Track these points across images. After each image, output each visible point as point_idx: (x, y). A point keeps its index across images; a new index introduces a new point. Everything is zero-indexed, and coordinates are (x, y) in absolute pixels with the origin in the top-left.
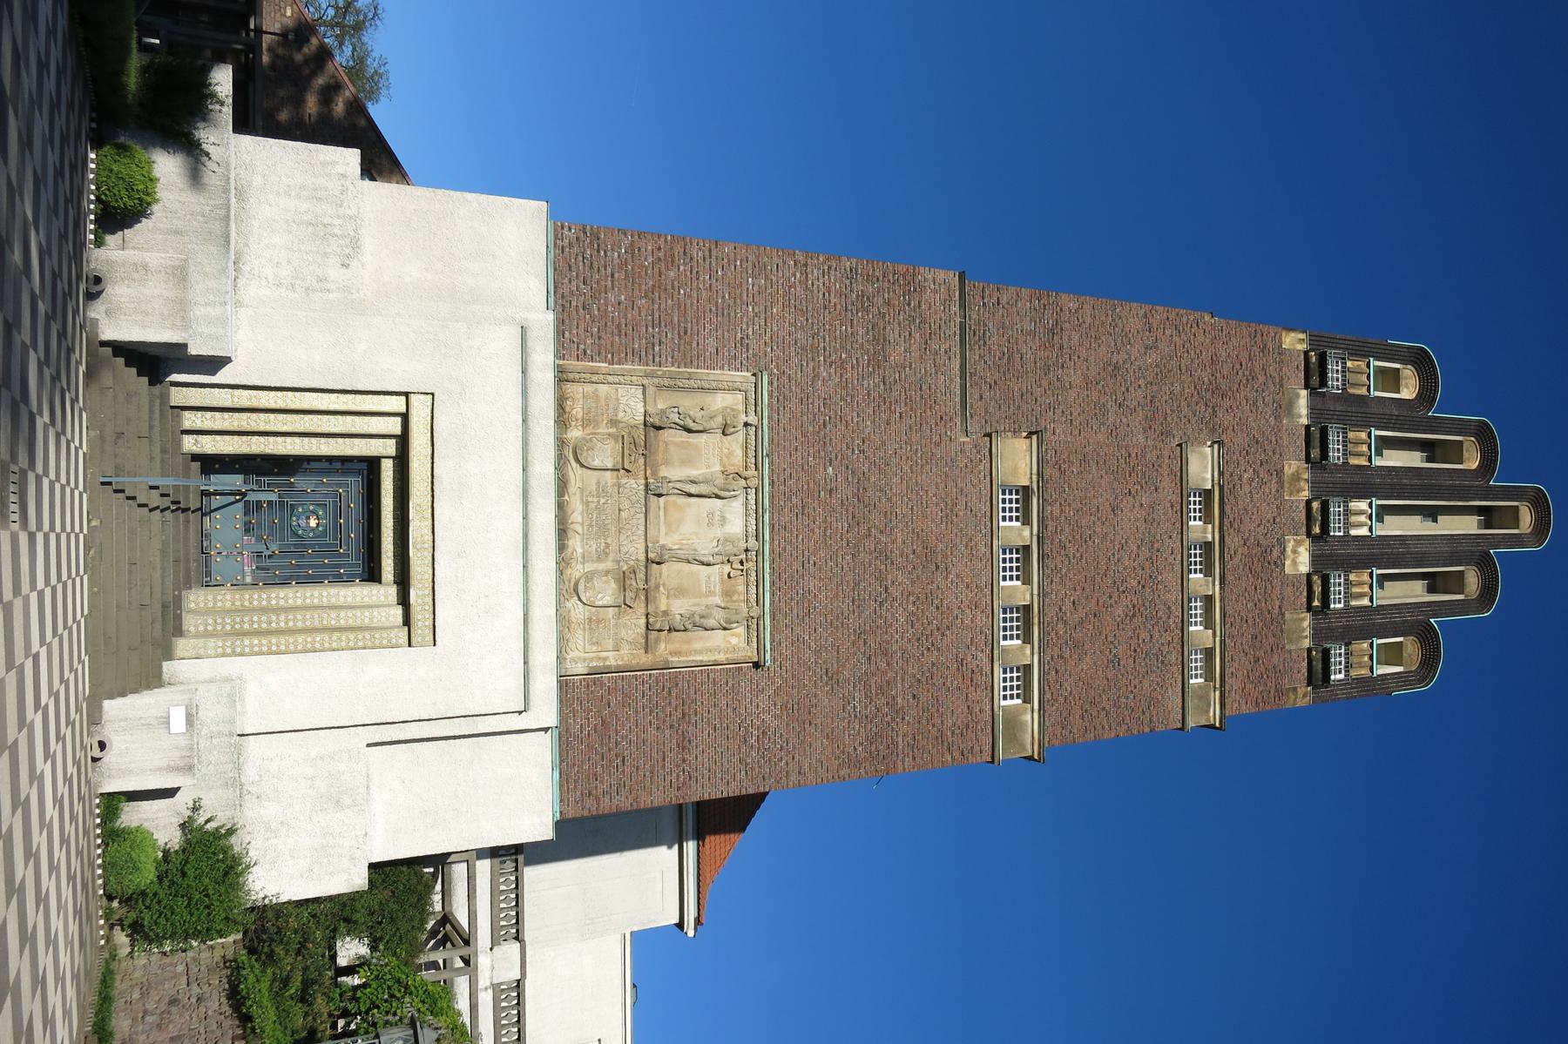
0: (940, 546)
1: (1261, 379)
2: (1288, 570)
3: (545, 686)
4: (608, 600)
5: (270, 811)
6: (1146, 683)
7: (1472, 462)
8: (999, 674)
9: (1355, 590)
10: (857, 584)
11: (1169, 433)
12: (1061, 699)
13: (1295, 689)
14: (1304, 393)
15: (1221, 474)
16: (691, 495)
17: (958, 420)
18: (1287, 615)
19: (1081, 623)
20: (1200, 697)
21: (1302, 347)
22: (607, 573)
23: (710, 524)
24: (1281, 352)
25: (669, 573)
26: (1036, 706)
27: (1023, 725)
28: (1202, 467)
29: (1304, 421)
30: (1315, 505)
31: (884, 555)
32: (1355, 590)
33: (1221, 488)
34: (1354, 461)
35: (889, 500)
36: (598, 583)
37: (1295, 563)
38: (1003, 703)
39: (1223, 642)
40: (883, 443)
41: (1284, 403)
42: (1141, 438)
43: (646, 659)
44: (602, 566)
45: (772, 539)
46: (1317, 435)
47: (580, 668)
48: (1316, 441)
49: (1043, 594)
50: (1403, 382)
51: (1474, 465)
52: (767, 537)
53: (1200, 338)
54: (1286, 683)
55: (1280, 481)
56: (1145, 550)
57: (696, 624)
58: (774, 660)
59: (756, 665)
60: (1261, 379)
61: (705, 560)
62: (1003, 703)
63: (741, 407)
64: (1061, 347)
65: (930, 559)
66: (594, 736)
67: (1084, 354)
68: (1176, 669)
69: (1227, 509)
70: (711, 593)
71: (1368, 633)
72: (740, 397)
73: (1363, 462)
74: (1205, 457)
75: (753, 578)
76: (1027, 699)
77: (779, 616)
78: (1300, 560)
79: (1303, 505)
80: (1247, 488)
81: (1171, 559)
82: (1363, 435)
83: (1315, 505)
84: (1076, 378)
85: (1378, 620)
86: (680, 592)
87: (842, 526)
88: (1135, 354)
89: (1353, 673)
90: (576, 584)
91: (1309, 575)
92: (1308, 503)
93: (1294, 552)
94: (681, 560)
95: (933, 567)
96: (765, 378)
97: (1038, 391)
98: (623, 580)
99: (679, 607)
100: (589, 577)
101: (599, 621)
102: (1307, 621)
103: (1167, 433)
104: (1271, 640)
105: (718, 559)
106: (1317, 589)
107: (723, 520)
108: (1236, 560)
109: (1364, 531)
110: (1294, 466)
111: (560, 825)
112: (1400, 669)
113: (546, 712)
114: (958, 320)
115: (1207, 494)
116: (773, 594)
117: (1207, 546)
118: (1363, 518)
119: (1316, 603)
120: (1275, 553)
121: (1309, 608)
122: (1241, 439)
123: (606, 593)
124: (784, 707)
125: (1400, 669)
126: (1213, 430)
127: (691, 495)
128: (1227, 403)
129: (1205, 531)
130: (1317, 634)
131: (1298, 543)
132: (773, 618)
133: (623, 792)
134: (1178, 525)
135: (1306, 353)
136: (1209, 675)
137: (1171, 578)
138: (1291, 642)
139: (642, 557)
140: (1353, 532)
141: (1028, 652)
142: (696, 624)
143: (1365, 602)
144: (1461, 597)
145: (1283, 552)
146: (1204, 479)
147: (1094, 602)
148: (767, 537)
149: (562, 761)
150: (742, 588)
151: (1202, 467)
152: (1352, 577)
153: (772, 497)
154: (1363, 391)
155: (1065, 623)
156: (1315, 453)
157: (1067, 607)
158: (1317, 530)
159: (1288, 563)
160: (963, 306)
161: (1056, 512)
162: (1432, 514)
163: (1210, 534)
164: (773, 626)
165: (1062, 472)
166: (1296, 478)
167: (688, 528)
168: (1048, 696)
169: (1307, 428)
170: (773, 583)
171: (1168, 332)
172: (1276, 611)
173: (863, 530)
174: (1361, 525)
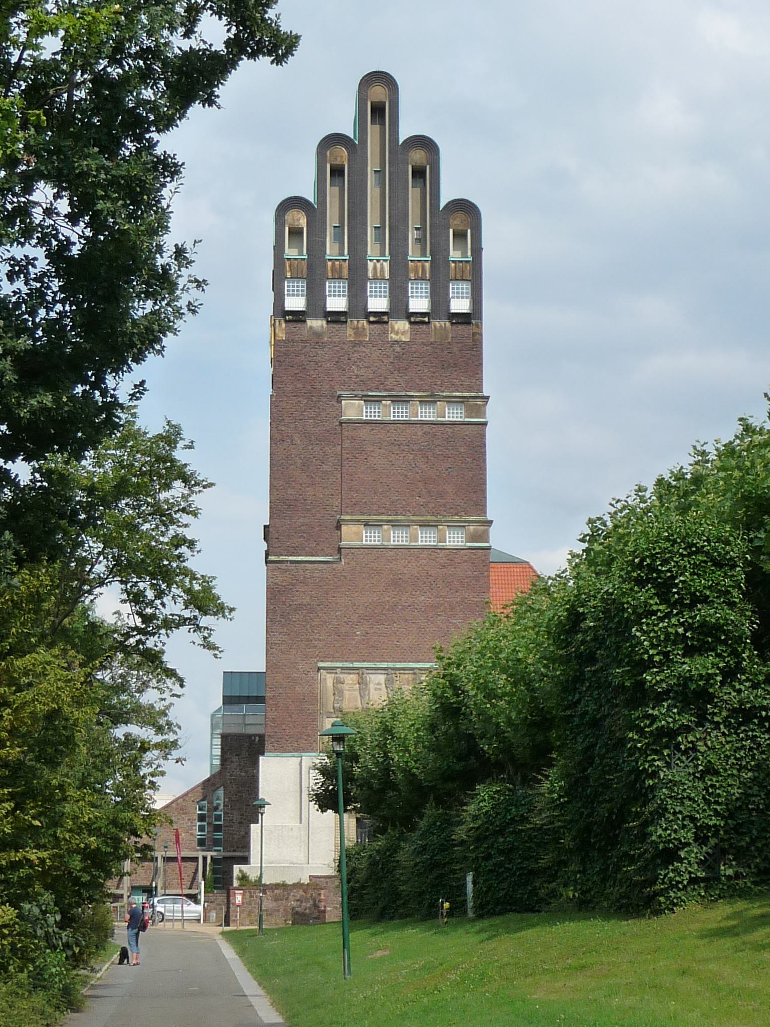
2: (405, 338)
15: (356, 396)
18: (432, 340)
21: (284, 325)
29: (324, 322)
30: (372, 319)
37: (403, 333)
52: (384, 665)
63: (333, 675)
72: (328, 675)
79: (372, 326)
80: (363, 371)
82: (330, 263)
91: (411, 323)
96: (321, 664)
104: (446, 352)
107: (379, 684)
109: (386, 265)
112: (469, 231)
118: (378, 265)
119: (426, 319)
120: (398, 349)
125: (469, 231)
129: (385, 406)
131: (393, 330)
135: (286, 321)
138: (447, 337)
146: (359, 405)
150: (406, 676)
157: (421, 501)
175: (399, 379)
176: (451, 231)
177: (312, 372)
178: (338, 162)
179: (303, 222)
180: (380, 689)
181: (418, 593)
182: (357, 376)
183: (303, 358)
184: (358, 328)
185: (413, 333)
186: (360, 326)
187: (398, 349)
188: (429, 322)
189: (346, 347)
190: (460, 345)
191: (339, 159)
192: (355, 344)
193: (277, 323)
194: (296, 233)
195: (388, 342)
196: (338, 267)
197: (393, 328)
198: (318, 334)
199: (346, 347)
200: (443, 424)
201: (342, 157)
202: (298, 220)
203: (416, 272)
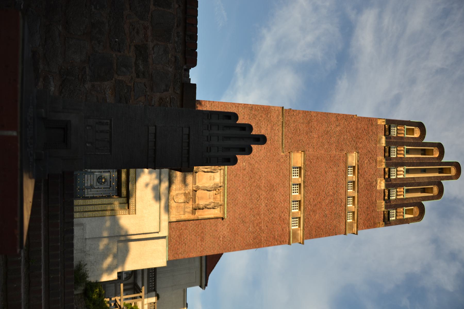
0: (275, 184)
2: (378, 188)
3: (165, 225)
4: (182, 201)
5: (92, 258)
6: (334, 222)
7: (436, 154)
8: (291, 220)
9: (399, 193)
10: (251, 195)
11: (343, 150)
12: (309, 227)
13: (379, 223)
14: (384, 137)
15: (358, 161)
16: (205, 172)
17: (281, 149)
18: (378, 201)
19: (315, 205)
21: (384, 123)
22: (182, 194)
23: (210, 179)
24: (377, 125)
25: (199, 193)
26: (302, 229)
27: (299, 233)
28: (353, 159)
30: (387, 169)
31: (259, 187)
32: (399, 193)
33: (358, 166)
34: (399, 156)
35: (261, 172)
36: (179, 197)
37: (380, 186)
38: (292, 228)
39: (358, 210)
40: (259, 156)
41: (378, 140)
42: (334, 152)
43: (192, 217)
44: (181, 192)
45: (227, 183)
46: (387, 150)
47: (174, 220)
48: (387, 150)
49: (304, 196)
50: (415, 132)
52: (226, 183)
53: (353, 122)
54: (377, 221)
55: (376, 162)
56: (335, 184)
57: (205, 207)
58: (227, 217)
59: (223, 219)
60: (371, 133)
61: (208, 189)
62: (292, 228)
64: (311, 127)
65: (271, 188)
66: (178, 238)
67: (318, 129)
68: (343, 218)
69: (360, 171)
70: (210, 198)
71: (402, 206)
73: (402, 156)
74: (353, 156)
75: (222, 194)
76: (299, 226)
77: (229, 205)
78: (382, 185)
79: (383, 170)
80: (366, 165)
81: (343, 186)
82: (402, 148)
83: (387, 169)
84: (315, 136)
85: (406, 202)
86: (202, 198)
87: (247, 179)
88: (333, 128)
89: (398, 218)
90: (173, 197)
91: (384, 190)
92: (384, 169)
93: (380, 183)
94: (202, 190)
95: (273, 190)
97: (304, 140)
98: (185, 194)
99: (202, 203)
100: (177, 195)
101: (179, 207)
102: (383, 203)
103: (342, 150)
105: (213, 189)
108: (362, 186)
109: (402, 176)
110: (381, 158)
111: (168, 262)
112: (412, 216)
113: (164, 232)
114: (281, 120)
115: (354, 167)
116: (227, 198)
117: (354, 182)
118: (402, 173)
119: (386, 198)
120: (374, 183)
121: (384, 199)
122: (365, 151)
123: (181, 199)
124: (230, 229)
126: (356, 149)
127: (205, 172)
128: (361, 140)
130: (386, 207)
131: (381, 180)
132: (227, 205)
133: (185, 253)
134: (345, 176)
135: (385, 125)
136: (353, 219)
137: (342, 191)
138: (378, 209)
139: (191, 189)
140: (399, 177)
141: (300, 213)
142: (205, 207)
143: (402, 197)
144: (432, 195)
145: (377, 183)
146: (353, 163)
147: (319, 199)
148: (226, 183)
149: (169, 244)
151: (353, 159)
152: (398, 190)
153: (228, 172)
154: (403, 135)
155: (311, 205)
156: (387, 154)
157: (312, 200)
158: (387, 177)
159: (378, 186)
160: (283, 116)
161: (309, 174)
162: (424, 171)
163: (355, 179)
164: (227, 207)
165: (311, 162)
166: (381, 161)
167: (204, 181)
168: (306, 226)
169: (385, 147)
170: (227, 195)
171: (343, 121)
172: (374, 200)
173: (253, 180)
174: (401, 174)
175: (363, 185)
176: (413, 207)
177: (365, 138)
178: (434, 153)
180: (210, 179)
181: (266, 202)
182: (364, 162)
185: (379, 192)
194: (411, 131)
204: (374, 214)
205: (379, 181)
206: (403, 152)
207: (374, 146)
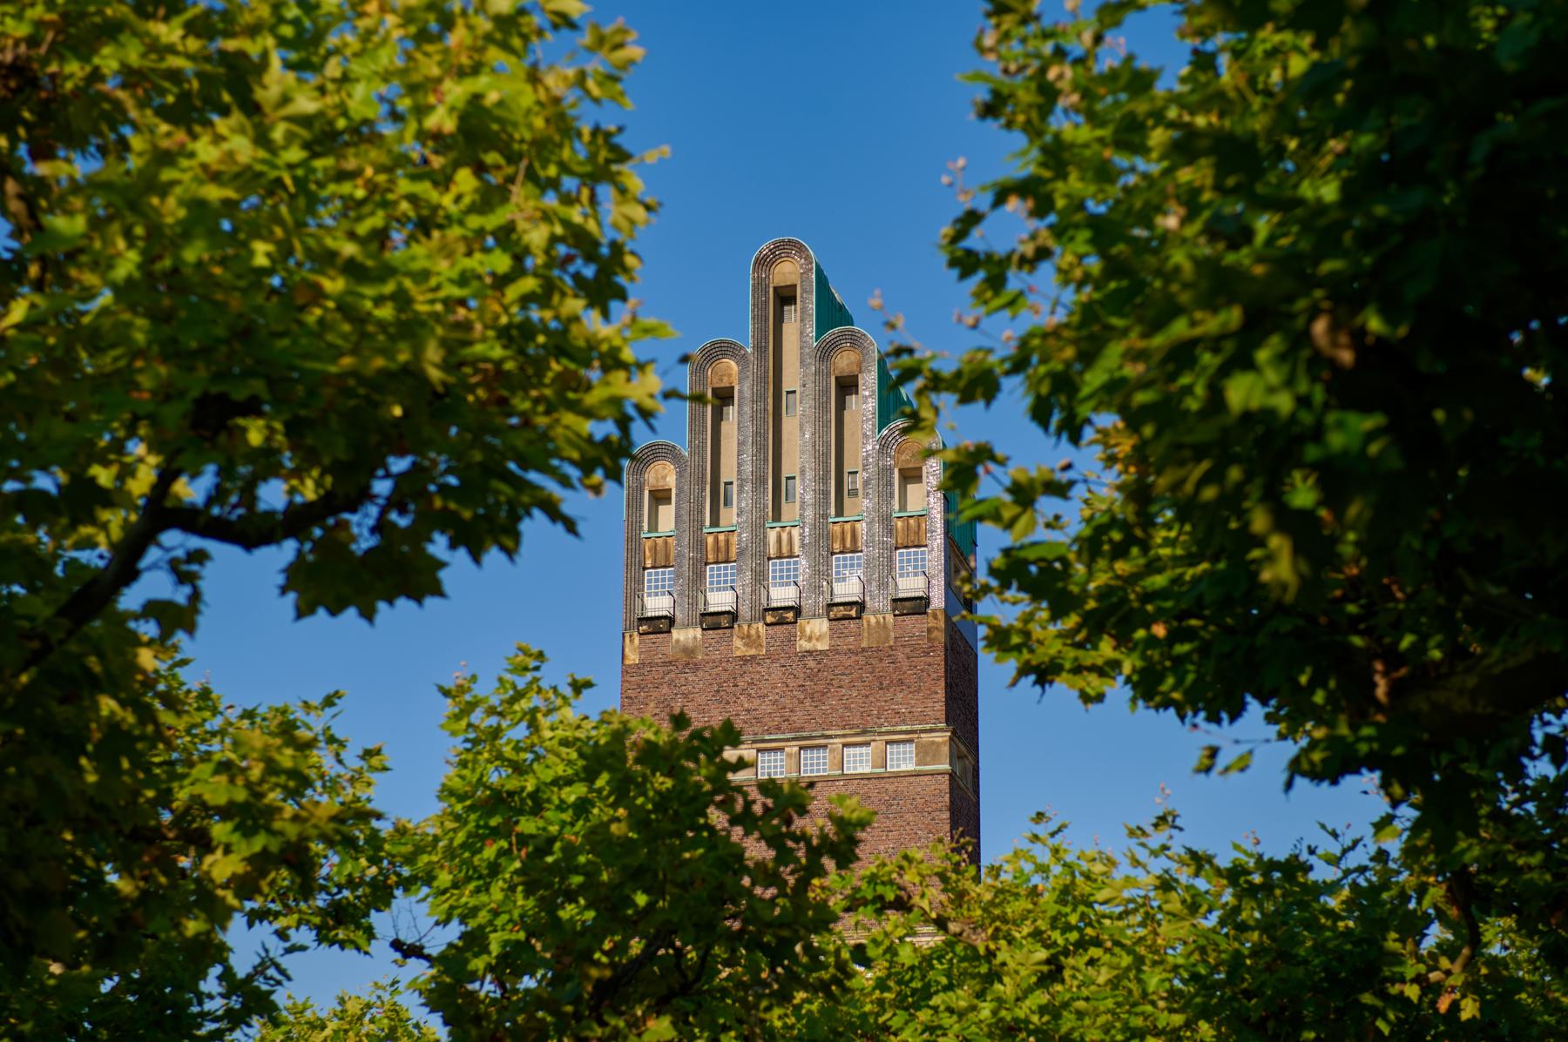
1: (665, 690)
2: (823, 646)
6: (909, 817)
9: (848, 545)
18: (864, 644)
20: (926, 753)
21: (637, 641)
29: (699, 630)
30: (769, 619)
33: (754, 742)
39: (880, 734)
51: (732, 365)
106: (841, 611)
118: (785, 536)
119: (853, 613)
158: (790, 615)
179: (671, 481)
183: (665, 690)
184: (749, 636)
186: (753, 632)
187: (812, 664)
188: (859, 617)
189: (730, 667)
190: (908, 650)
191: (725, 379)
192: (745, 660)
193: (627, 639)
195: (796, 654)
196: (722, 544)
197: (803, 631)
198: (689, 651)
199: (730, 667)
200: (879, 778)
201: (730, 375)
202: (664, 478)
203: (843, 540)
204: (900, 656)
205: (806, 645)
206: (722, 537)
207: (701, 674)
